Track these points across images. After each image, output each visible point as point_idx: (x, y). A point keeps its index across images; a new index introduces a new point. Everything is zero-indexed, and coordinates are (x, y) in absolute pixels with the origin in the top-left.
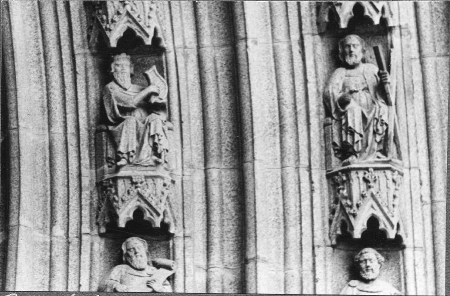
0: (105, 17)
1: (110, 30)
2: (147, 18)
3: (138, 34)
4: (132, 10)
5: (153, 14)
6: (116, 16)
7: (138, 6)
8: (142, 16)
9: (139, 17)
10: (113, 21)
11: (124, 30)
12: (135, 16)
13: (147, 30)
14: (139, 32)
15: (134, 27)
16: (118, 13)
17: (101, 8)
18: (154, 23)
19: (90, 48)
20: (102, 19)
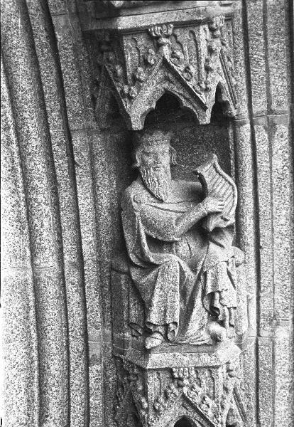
0: (119, 71)
1: (131, 98)
2: (203, 70)
3: (185, 103)
4: (173, 55)
5: (215, 64)
6: (140, 69)
7: (186, 48)
8: (193, 69)
9: (187, 70)
10: (135, 80)
11: (159, 95)
12: (179, 69)
13: (203, 97)
14: (187, 100)
15: (176, 90)
16: (146, 64)
17: (112, 50)
18: (217, 78)
19: (96, 119)
20: (115, 72)
